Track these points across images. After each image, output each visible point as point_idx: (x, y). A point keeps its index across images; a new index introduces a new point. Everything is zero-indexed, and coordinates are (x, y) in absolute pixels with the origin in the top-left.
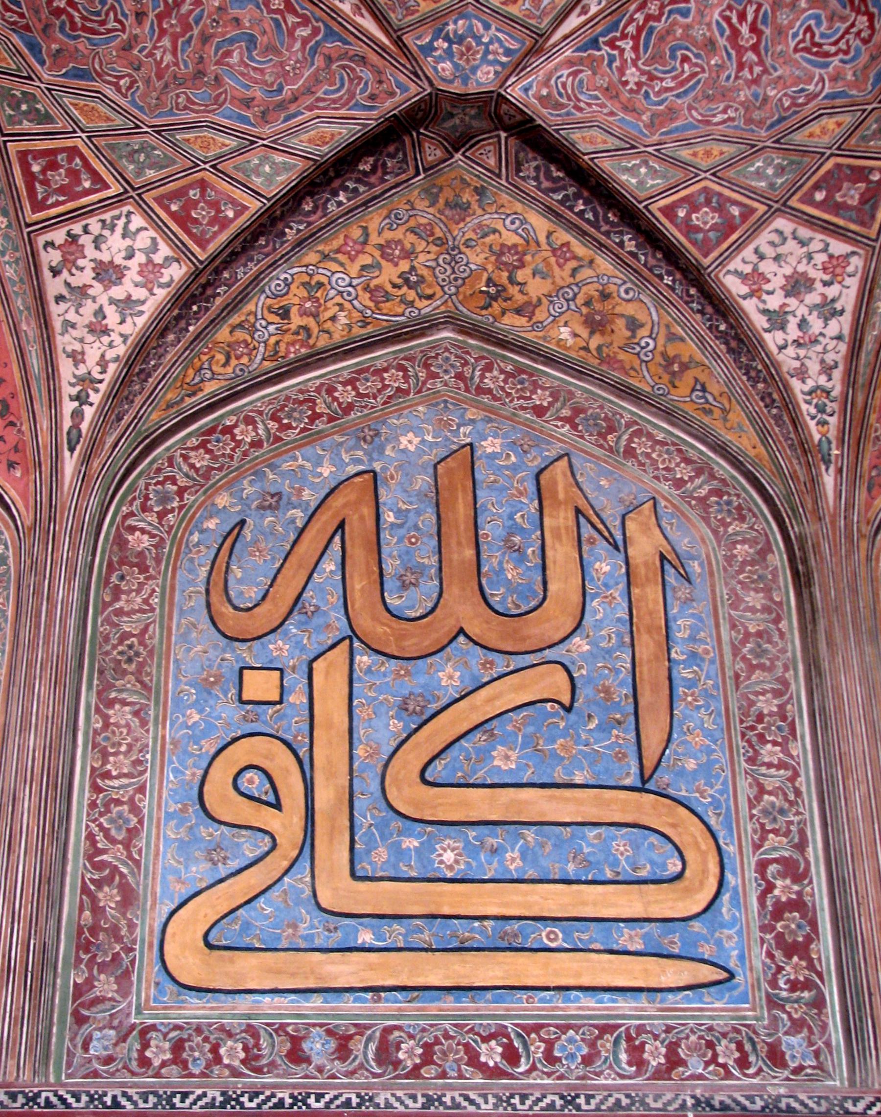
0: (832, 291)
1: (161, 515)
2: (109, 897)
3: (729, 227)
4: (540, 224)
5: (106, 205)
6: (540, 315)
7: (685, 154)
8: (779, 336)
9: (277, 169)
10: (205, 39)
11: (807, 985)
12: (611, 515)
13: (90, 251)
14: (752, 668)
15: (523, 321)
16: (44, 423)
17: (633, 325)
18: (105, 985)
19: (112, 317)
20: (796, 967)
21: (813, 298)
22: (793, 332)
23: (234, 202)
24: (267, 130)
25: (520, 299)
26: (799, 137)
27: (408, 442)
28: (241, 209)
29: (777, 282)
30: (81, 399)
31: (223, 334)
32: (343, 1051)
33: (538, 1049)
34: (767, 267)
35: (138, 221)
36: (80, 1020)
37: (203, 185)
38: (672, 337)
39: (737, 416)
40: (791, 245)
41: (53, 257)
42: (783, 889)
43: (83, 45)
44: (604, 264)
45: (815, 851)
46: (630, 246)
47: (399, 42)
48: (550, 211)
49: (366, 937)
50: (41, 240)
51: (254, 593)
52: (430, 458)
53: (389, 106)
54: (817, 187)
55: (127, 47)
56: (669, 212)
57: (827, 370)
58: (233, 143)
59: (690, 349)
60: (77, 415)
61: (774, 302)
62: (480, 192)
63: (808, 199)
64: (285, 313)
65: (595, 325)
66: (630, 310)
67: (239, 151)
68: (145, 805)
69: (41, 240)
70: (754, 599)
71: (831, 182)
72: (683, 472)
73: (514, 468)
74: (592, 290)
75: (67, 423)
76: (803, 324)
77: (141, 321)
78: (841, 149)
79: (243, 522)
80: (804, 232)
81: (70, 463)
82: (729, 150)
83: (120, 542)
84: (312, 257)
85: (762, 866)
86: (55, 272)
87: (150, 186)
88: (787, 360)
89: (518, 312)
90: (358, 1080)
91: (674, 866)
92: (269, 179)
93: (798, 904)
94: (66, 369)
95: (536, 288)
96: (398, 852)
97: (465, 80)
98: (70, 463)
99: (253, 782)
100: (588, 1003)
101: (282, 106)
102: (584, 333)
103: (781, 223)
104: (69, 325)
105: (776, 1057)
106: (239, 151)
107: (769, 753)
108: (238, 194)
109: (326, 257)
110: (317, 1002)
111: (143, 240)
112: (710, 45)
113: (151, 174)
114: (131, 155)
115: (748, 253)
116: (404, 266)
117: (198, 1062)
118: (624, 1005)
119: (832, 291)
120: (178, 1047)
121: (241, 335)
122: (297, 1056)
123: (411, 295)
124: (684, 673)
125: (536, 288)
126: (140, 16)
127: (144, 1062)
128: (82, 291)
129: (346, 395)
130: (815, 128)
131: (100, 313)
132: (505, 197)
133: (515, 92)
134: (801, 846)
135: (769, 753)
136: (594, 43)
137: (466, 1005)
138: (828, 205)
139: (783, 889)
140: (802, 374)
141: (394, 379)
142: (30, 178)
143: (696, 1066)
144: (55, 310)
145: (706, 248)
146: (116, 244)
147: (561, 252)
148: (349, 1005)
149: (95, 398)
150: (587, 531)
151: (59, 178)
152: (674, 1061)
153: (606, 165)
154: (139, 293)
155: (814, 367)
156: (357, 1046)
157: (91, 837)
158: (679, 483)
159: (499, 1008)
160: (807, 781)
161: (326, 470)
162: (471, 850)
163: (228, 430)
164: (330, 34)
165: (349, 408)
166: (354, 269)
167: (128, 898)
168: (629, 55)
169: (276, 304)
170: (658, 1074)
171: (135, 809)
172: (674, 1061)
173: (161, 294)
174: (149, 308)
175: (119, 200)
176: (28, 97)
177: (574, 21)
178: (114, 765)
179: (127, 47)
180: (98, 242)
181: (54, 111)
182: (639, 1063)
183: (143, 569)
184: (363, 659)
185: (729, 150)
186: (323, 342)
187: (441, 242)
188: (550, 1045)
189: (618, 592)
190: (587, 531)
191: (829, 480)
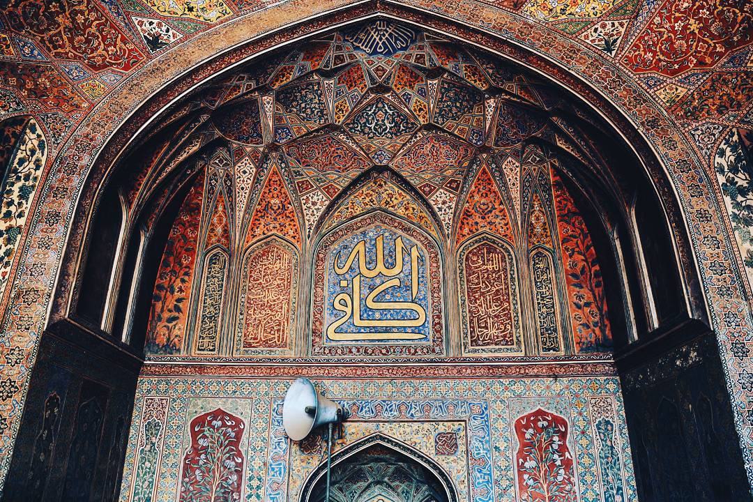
0: (451, 204)
1: (325, 250)
2: (318, 323)
3: (431, 191)
4: (396, 189)
5: (313, 190)
6: (396, 207)
7: (423, 176)
8: (441, 213)
9: (346, 181)
10: (331, 156)
11: (440, 338)
12: (409, 247)
13: (311, 200)
14: (433, 278)
15: (392, 209)
16: (303, 234)
17: (414, 209)
18: (317, 340)
19: (315, 211)
20: (438, 335)
21: (447, 205)
22: (443, 212)
23: (337, 188)
24: (344, 174)
25: (392, 204)
26: (445, 173)
27: (371, 234)
28: (339, 190)
29: (440, 202)
30: (310, 228)
31: (336, 214)
32: (358, 351)
33: (392, 350)
34: (438, 199)
35: (319, 193)
36: (313, 346)
37: (331, 185)
38: (421, 212)
39: (433, 228)
40: (443, 194)
41: (304, 201)
42: (437, 320)
43: (308, 160)
44: (408, 197)
45: (443, 314)
46: (413, 193)
47: (367, 155)
48: (398, 187)
49: (362, 330)
50: (301, 199)
51: (342, 265)
52: (376, 237)
53: (366, 168)
54: (448, 183)
55: (317, 159)
56: (420, 188)
57: (449, 220)
58: (337, 177)
59: (424, 214)
60: (309, 231)
61: (440, 206)
62: (385, 183)
63: (446, 186)
64: (347, 209)
65: (407, 209)
66: (413, 206)
67: (338, 178)
68: (323, 306)
69: (301, 199)
70: (435, 265)
71: (451, 182)
72: (422, 239)
73: (391, 239)
74: (406, 202)
75: (307, 233)
76: (445, 210)
77: (321, 213)
78: (452, 176)
79: (340, 251)
80: (445, 192)
81: (308, 241)
82: (432, 175)
83: (318, 256)
84: (352, 197)
85: (433, 316)
86: (304, 204)
87: (322, 186)
88: (442, 218)
89: (392, 207)
90: (361, 356)
91: (417, 317)
92: (344, 183)
93: (439, 323)
94: (307, 223)
95: (395, 202)
96: (369, 315)
97: (381, 163)
98: (308, 241)
99: (342, 302)
100: (401, 342)
101: (346, 169)
102: (404, 211)
103: (442, 191)
104: (307, 214)
105: (434, 351)
106: (338, 178)
107: (435, 295)
108: (338, 186)
109: (355, 197)
110: (354, 342)
111: (320, 197)
112: (428, 155)
113: (322, 184)
114: (318, 180)
115: (435, 196)
116: (370, 198)
117: (333, 353)
118: (408, 342)
119: (451, 204)
120: (330, 350)
121: (339, 214)
122: (351, 352)
123: (372, 204)
124: (421, 279)
125: (395, 202)
126: (319, 154)
127: (325, 353)
128: (309, 208)
129: (359, 225)
130: (447, 172)
131: (313, 211)
132: (389, 184)
133: (390, 165)
134: (440, 313)
135: (435, 295)
136: (405, 155)
137: (380, 343)
138: (450, 187)
139: (437, 320)
140: (444, 220)
141: (368, 221)
142: (299, 187)
143: (420, 353)
144: (305, 212)
145: (427, 196)
146: (315, 197)
147: (400, 194)
148: (359, 343)
149: (312, 228)
150: (404, 252)
151: (304, 186)
152: (416, 352)
153: (408, 179)
154: (320, 207)
155: (447, 219)
156: (361, 350)
157: (314, 313)
158: (421, 241)
159: (386, 343)
160: (442, 300)
161: (356, 240)
162: (381, 315)
163: (337, 233)
164: (355, 155)
165: (360, 227)
166: (361, 199)
167: (321, 324)
168: (412, 157)
169: (346, 207)
170: (413, 354)
171: (322, 307)
172: (416, 352)
173: (324, 207)
174: (322, 210)
175: (316, 189)
176: (298, 171)
177: (402, 151)
178: (319, 299)
179: (317, 159)
180: (312, 198)
181: (303, 173)
182: (410, 352)
183: (322, 261)
184: (362, 278)
185: (432, 175)
186: (355, 214)
187: (377, 193)
188: (394, 350)
189: (409, 264)
190: (404, 252)
191: (449, 241)
